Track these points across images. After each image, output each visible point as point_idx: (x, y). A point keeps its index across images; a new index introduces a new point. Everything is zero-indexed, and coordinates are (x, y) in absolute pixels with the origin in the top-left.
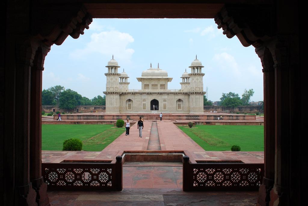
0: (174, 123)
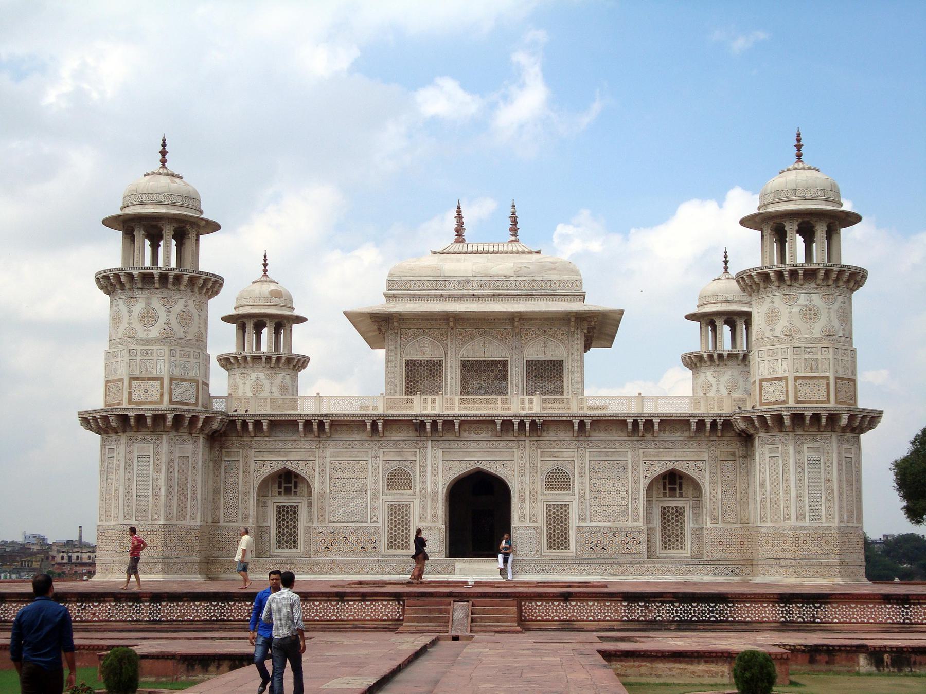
0: (599, 651)
